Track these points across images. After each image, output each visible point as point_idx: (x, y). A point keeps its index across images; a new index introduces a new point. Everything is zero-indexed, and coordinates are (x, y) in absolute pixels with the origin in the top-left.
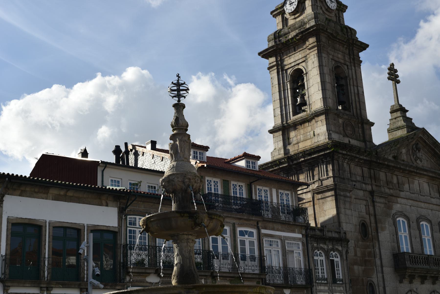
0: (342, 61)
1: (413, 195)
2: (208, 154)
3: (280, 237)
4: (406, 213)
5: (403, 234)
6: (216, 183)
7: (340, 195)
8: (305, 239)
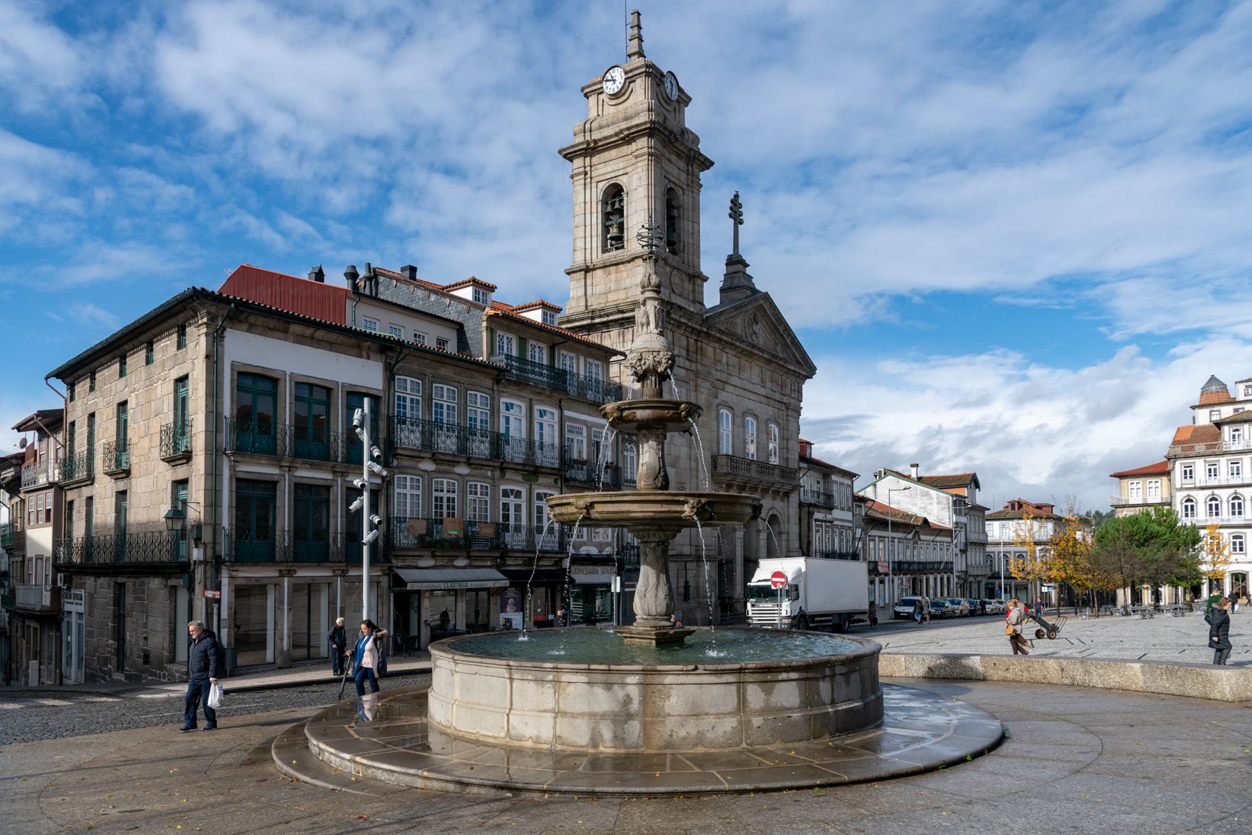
2: (494, 296)
5: (726, 428)
6: (510, 341)
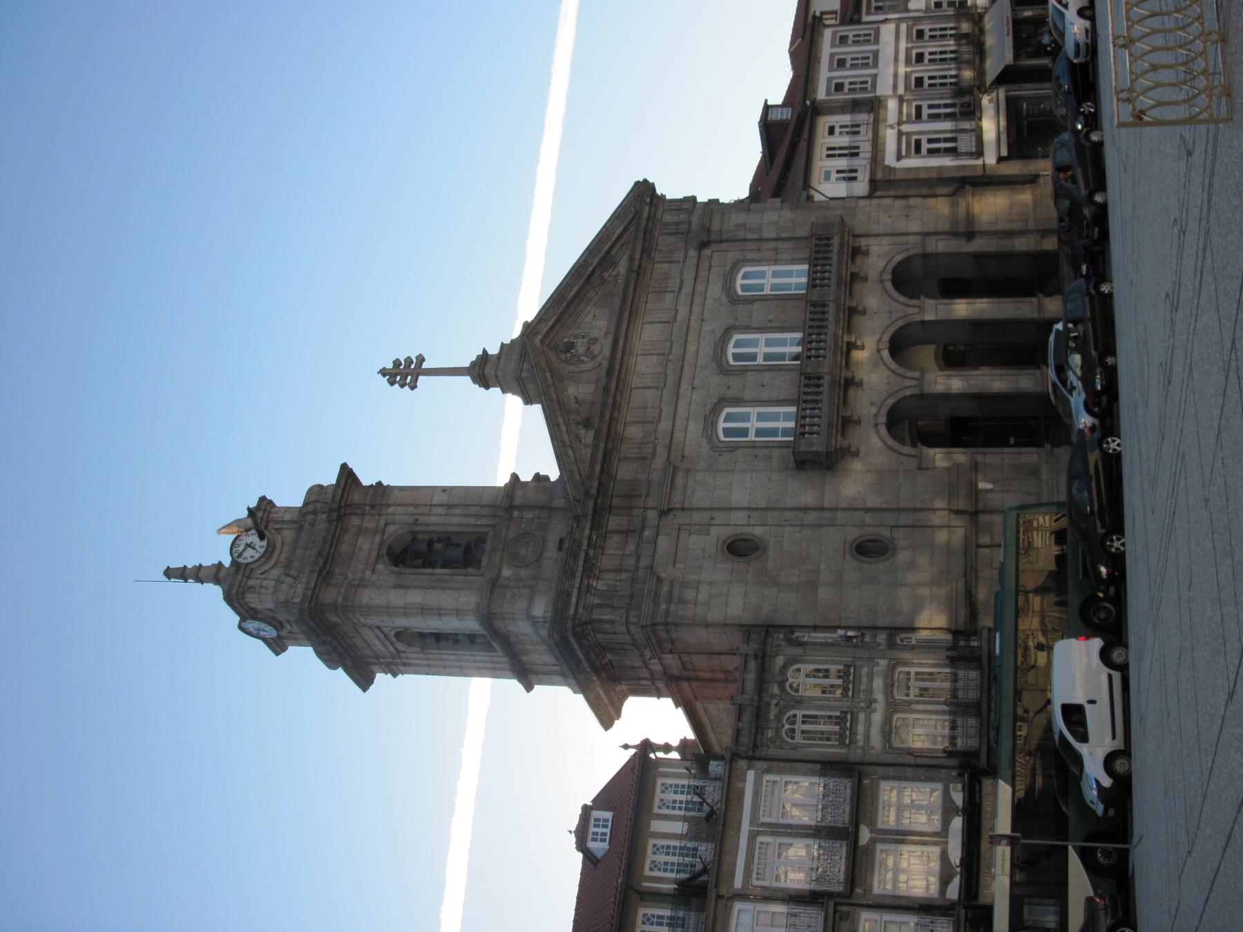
0: (378, 539)
1: (670, 379)
3: (752, 836)
4: (709, 407)
7: (667, 612)
8: (760, 764)
